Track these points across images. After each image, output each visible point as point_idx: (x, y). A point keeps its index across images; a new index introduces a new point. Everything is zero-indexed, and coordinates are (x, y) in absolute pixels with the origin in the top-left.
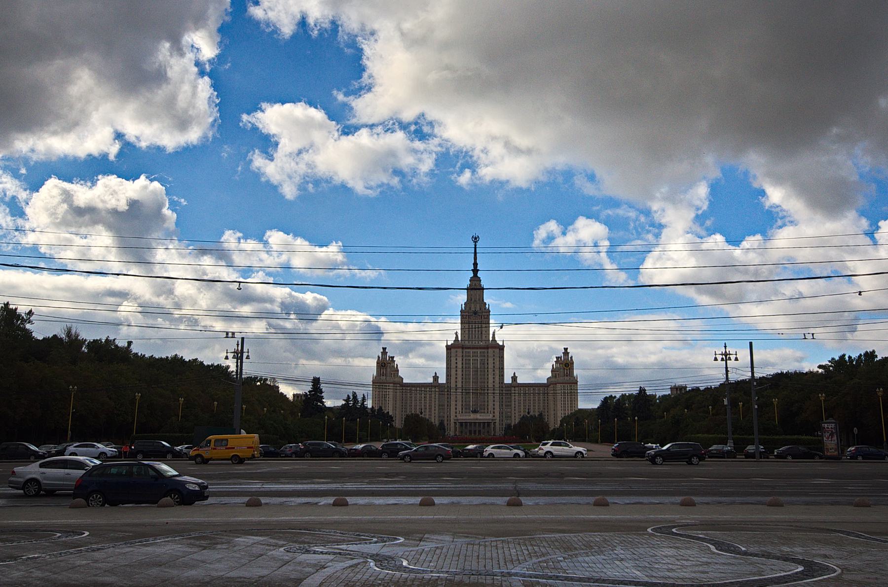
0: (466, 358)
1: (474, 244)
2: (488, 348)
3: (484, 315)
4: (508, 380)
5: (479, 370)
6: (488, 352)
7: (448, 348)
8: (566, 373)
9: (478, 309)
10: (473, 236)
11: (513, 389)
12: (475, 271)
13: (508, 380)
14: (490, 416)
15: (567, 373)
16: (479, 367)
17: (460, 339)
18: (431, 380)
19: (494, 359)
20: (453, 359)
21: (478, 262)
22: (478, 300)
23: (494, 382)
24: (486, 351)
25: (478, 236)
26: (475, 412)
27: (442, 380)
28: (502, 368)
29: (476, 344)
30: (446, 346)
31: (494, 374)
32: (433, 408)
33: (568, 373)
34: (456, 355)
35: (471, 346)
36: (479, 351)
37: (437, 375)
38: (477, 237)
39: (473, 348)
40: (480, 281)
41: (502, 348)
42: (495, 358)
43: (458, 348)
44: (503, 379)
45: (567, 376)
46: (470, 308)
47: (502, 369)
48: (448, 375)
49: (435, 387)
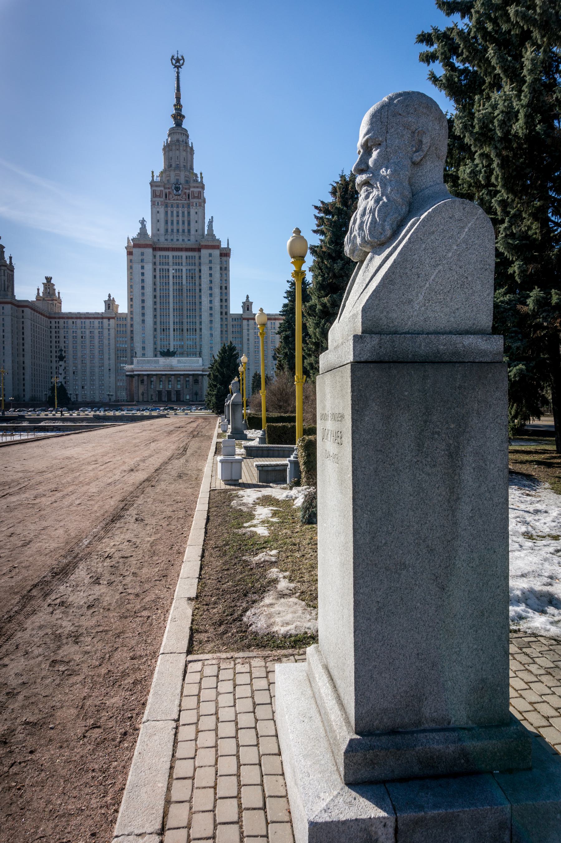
1: (176, 69)
2: (199, 250)
3: (193, 192)
5: (185, 287)
6: (200, 258)
9: (182, 180)
10: (173, 57)
11: (245, 322)
12: (178, 117)
13: (236, 308)
14: (198, 363)
16: (184, 282)
18: (101, 309)
19: (211, 268)
21: (182, 102)
23: (211, 308)
24: (196, 254)
25: (182, 57)
26: (168, 354)
27: (123, 308)
28: (226, 288)
29: (180, 240)
31: (211, 295)
32: (106, 356)
34: (142, 261)
36: (184, 254)
37: (112, 298)
38: (180, 58)
39: (174, 249)
40: (188, 136)
41: (226, 254)
42: (212, 265)
43: (146, 246)
44: (227, 307)
47: (225, 289)
48: (131, 300)
49: (109, 319)
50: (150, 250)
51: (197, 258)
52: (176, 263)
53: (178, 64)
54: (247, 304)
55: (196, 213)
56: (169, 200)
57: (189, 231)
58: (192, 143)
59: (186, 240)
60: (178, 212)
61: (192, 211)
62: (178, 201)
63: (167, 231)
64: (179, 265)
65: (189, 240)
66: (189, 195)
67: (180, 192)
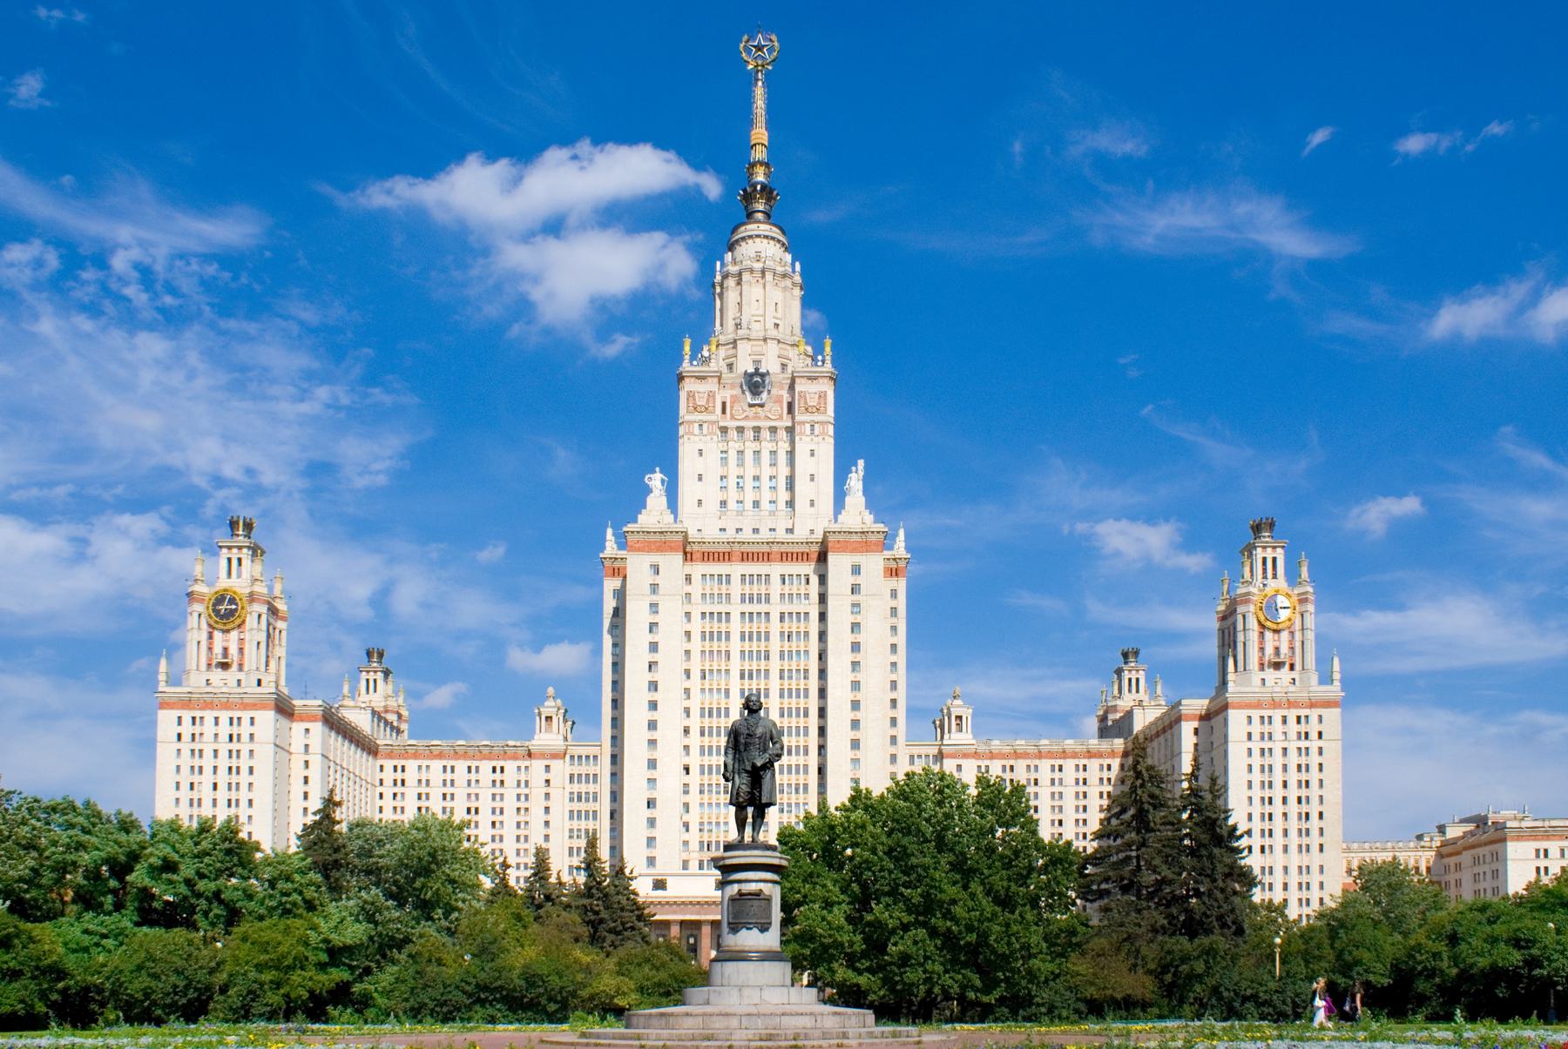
0: (708, 609)
2: (822, 558)
6: (823, 579)
8: (1269, 651)
15: (1277, 649)
22: (770, 325)
33: (1284, 650)
34: (654, 588)
35: (736, 547)
36: (776, 569)
39: (746, 557)
45: (1277, 666)
46: (730, 366)
50: (680, 557)
52: (751, 595)
55: (812, 453)
56: (733, 417)
57: (791, 504)
63: (723, 503)
64: (759, 601)
67: (764, 395)
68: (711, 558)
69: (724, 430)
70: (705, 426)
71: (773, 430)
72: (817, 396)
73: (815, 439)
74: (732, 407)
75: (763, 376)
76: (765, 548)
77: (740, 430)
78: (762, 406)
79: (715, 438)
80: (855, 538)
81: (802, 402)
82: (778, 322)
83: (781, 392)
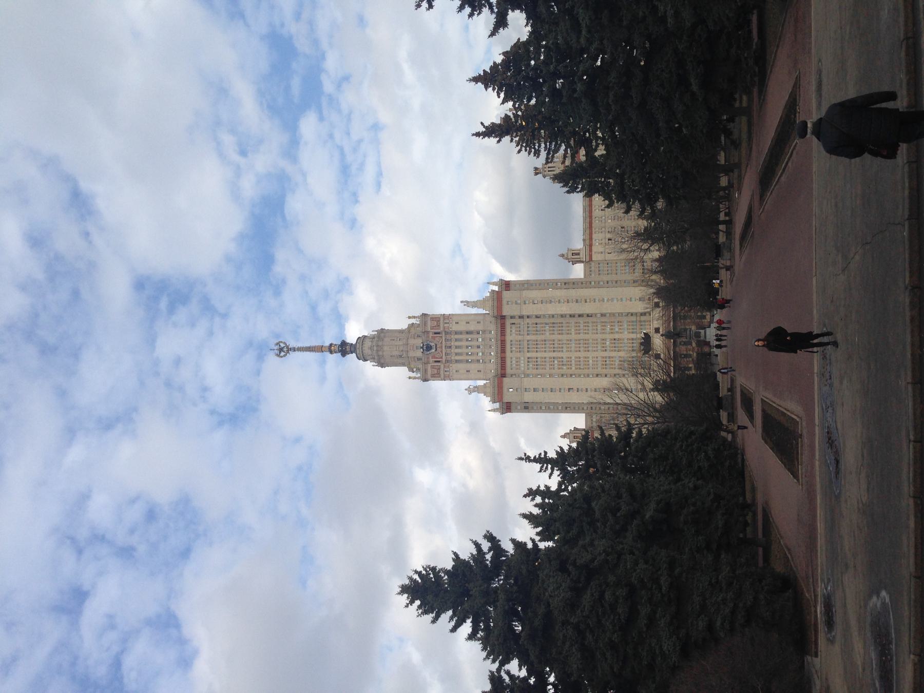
2: (503, 318)
4: (578, 271)
6: (512, 317)
7: (507, 408)
10: (278, 355)
12: (344, 349)
13: (578, 271)
17: (481, 383)
20: (529, 397)
22: (401, 343)
24: (508, 322)
25: (278, 344)
30: (502, 413)
36: (508, 338)
38: (277, 347)
39: (503, 350)
41: (506, 285)
46: (419, 359)
51: (513, 321)
53: (285, 349)
54: (570, 256)
55: (457, 323)
56: (442, 358)
58: (373, 331)
59: (491, 336)
60: (457, 347)
61: (455, 328)
62: (444, 346)
65: (490, 332)
66: (435, 333)
67: (432, 344)
68: (504, 366)
69: (447, 361)
70: (446, 369)
71: (446, 340)
72: (433, 322)
73: (451, 322)
74: (437, 358)
75: (423, 345)
76: (499, 342)
77: (446, 354)
78: (436, 345)
79: (451, 365)
80: (496, 304)
81: (435, 328)
82: (398, 339)
83: (430, 337)
